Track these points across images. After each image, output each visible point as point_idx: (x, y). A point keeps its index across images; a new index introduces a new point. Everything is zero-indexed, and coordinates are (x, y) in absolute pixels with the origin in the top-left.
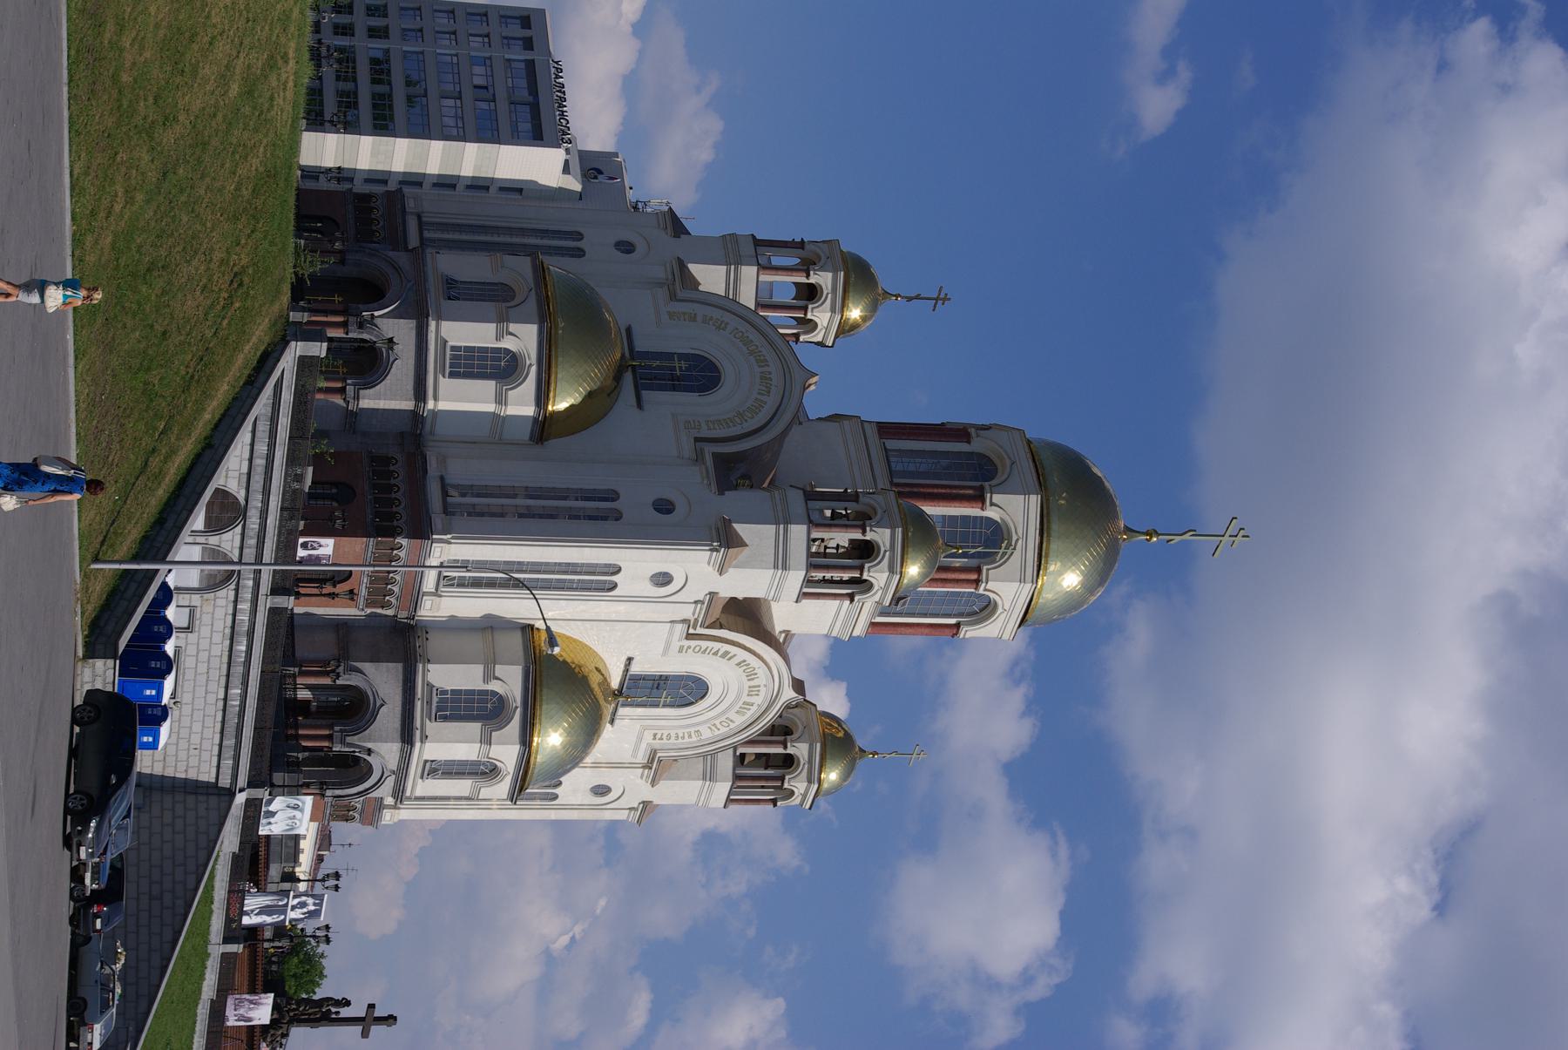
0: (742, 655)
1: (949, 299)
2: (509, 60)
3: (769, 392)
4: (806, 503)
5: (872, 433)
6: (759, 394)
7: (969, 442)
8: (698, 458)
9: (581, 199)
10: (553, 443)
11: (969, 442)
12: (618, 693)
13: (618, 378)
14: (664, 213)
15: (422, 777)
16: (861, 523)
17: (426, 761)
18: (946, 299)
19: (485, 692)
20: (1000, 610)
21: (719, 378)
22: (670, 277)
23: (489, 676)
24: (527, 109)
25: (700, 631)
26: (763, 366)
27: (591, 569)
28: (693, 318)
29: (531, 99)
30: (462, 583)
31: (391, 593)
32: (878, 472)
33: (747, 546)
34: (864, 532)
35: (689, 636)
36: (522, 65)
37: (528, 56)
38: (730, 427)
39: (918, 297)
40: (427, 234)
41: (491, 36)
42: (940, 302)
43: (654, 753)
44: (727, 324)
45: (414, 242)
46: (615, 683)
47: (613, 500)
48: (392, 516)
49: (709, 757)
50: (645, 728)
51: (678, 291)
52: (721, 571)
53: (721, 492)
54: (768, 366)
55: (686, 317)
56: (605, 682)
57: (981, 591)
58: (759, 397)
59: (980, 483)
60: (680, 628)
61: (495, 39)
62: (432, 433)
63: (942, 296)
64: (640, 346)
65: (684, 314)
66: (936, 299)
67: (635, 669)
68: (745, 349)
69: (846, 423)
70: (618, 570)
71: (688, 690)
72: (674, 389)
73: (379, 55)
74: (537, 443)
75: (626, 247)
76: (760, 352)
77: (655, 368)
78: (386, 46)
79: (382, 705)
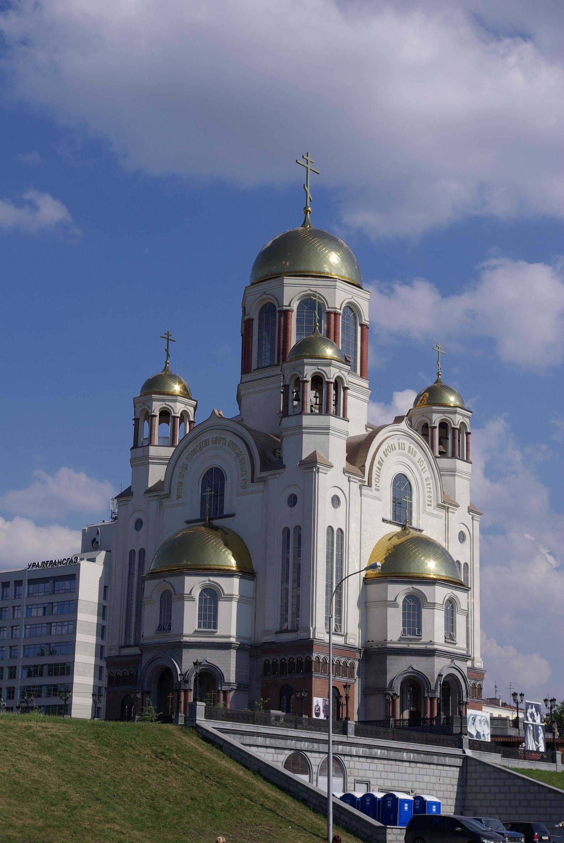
0: (380, 454)
1: (168, 332)
2: (28, 595)
3: (224, 439)
4: (290, 416)
5: (247, 377)
6: (225, 445)
7: (253, 320)
8: (263, 480)
9: (110, 551)
10: (255, 567)
11: (253, 320)
12: (404, 527)
13: (216, 528)
14: (118, 502)
15: (455, 644)
17: (445, 642)
18: (168, 334)
19: (404, 606)
20: (352, 300)
21: (215, 468)
22: (156, 498)
23: (394, 604)
24: (57, 583)
26: (209, 442)
27: (330, 544)
28: (181, 484)
29: (51, 581)
30: (339, 621)
31: (345, 663)
32: (272, 373)
33: (315, 451)
34: (307, 381)
35: (370, 485)
36: (31, 586)
37: (25, 583)
39: (167, 351)
40: (132, 643)
41: (13, 605)
42: (170, 337)
43: (439, 506)
45: (136, 651)
46: (398, 529)
47: (289, 530)
49: (441, 473)
51: (164, 493)
52: (331, 466)
53: (283, 467)
54: (208, 439)
55: (180, 488)
56: (397, 535)
57: (341, 312)
58: (227, 444)
60: (365, 491)
61: (16, 603)
62: (250, 639)
63: (166, 336)
64: (197, 515)
65: (178, 489)
66: (168, 339)
67: (389, 517)
68: (198, 453)
69: (242, 393)
70: (330, 528)
72: (222, 495)
73: (26, 672)
74: (255, 576)
75: (139, 524)
76: (200, 444)
77: (210, 506)
78: (21, 668)
79: (412, 668)
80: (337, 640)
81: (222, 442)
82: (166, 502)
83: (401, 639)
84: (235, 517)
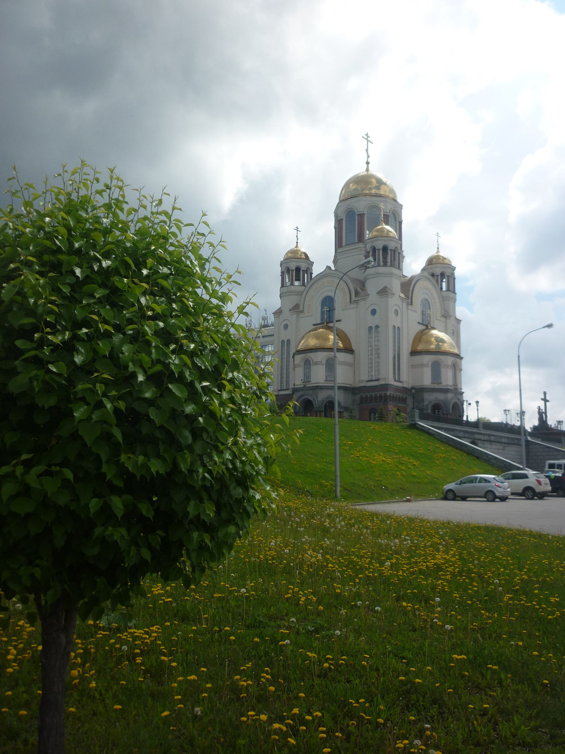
5: (339, 250)
8: (356, 302)
10: (354, 348)
11: (342, 219)
16: (377, 251)
18: (297, 228)
23: (427, 365)
25: (410, 301)
30: (399, 375)
31: (402, 396)
32: (355, 247)
35: (412, 304)
39: (297, 237)
43: (443, 316)
48: (381, 397)
50: (437, 319)
52: (394, 294)
57: (390, 214)
60: (410, 307)
64: (319, 321)
70: (394, 326)
71: (426, 304)
75: (286, 327)
80: (399, 384)
82: (301, 315)
83: (432, 383)
84: (341, 322)
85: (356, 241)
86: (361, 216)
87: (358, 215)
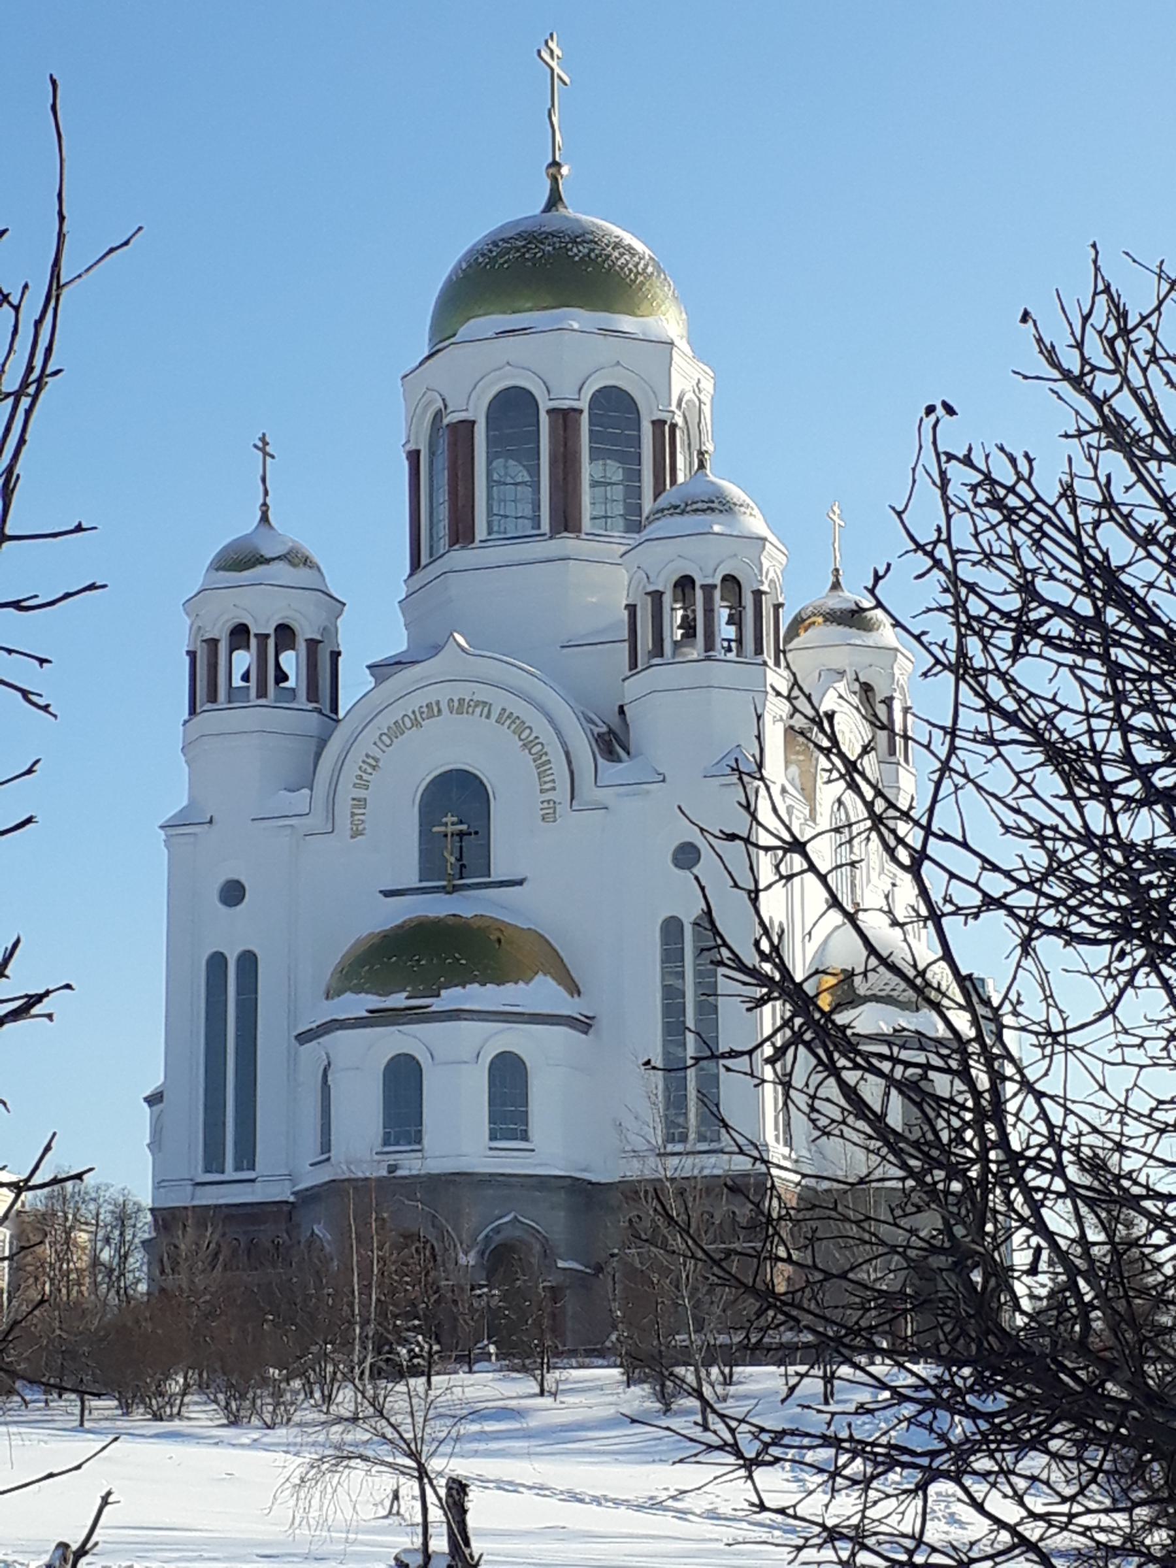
6: (488, 717)
28: (361, 802)
38: (535, 761)
44: (367, 756)
55: (356, 811)
58: (494, 716)
59: (544, 419)
65: (353, 814)
66: (265, 454)
75: (233, 893)
81: (478, 710)
85: (545, 527)
86: (565, 418)
87: (550, 412)
